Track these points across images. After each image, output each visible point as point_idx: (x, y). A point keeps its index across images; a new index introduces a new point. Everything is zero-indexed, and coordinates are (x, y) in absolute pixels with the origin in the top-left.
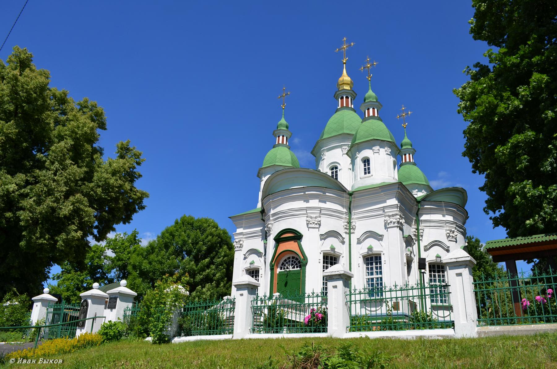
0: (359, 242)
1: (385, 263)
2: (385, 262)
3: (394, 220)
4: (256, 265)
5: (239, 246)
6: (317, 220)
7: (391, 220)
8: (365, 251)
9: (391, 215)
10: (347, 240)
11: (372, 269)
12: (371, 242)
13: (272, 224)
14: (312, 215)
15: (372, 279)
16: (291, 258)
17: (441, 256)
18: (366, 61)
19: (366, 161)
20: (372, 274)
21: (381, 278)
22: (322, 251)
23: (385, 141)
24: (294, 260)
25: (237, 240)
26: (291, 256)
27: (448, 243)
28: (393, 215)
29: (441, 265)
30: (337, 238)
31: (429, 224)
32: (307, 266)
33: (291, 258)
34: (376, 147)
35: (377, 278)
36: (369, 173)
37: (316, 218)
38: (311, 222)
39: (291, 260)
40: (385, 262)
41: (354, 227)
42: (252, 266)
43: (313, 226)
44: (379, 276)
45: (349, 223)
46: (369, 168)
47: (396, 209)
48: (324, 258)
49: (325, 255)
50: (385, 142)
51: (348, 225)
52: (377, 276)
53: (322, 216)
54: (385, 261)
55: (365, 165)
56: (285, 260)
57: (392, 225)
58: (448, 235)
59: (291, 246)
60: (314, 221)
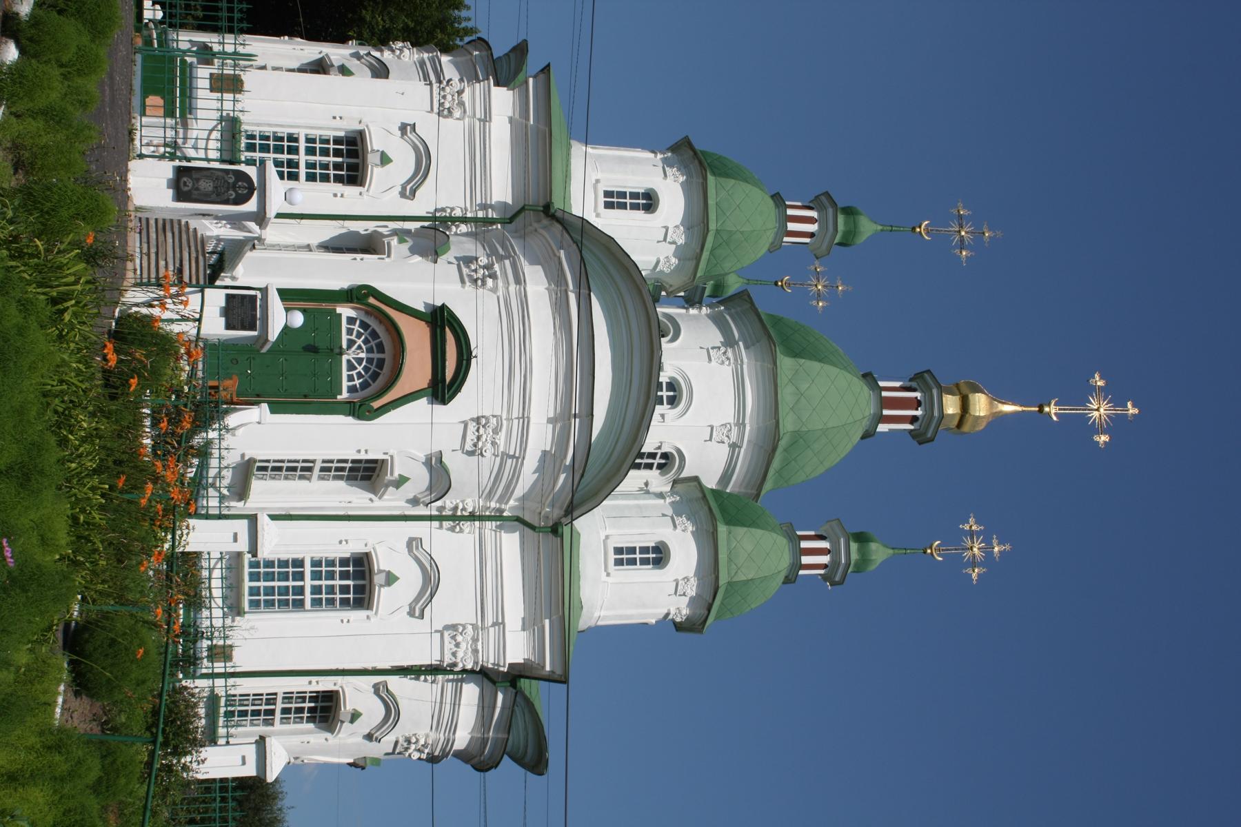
0: (413, 544)
1: (342, 621)
2: (345, 621)
3: (460, 654)
4: (376, 174)
5: (447, 105)
6: (489, 445)
7: (463, 646)
8: (382, 562)
9: (476, 646)
10: (421, 511)
11: (331, 576)
12: (410, 580)
13: (494, 290)
14: (503, 434)
15: (300, 576)
16: (381, 356)
17: (355, 724)
18: (995, 542)
19: (658, 556)
20: (316, 576)
21: (299, 605)
22: (392, 457)
23: (709, 610)
24: (373, 368)
25: (466, 96)
26: (388, 346)
27: (389, 740)
28: (475, 651)
29: (332, 715)
30: (430, 488)
31: (448, 701)
32: (350, 419)
33: (381, 356)
34: (694, 588)
35: (300, 591)
36: (619, 562)
37: (494, 444)
38: (482, 431)
39: (376, 356)
40: (345, 621)
41: (458, 529)
42: (372, 159)
43: (471, 437)
44: (308, 597)
45: (472, 517)
46: (632, 562)
47: (492, 661)
48: (368, 461)
49: (378, 466)
50: (706, 612)
51: (466, 514)
52: (308, 590)
53: (498, 459)
54: (348, 621)
55: (644, 550)
56: (374, 335)
57: (449, 646)
58: (414, 740)
59: (417, 370)
60: (484, 438)
